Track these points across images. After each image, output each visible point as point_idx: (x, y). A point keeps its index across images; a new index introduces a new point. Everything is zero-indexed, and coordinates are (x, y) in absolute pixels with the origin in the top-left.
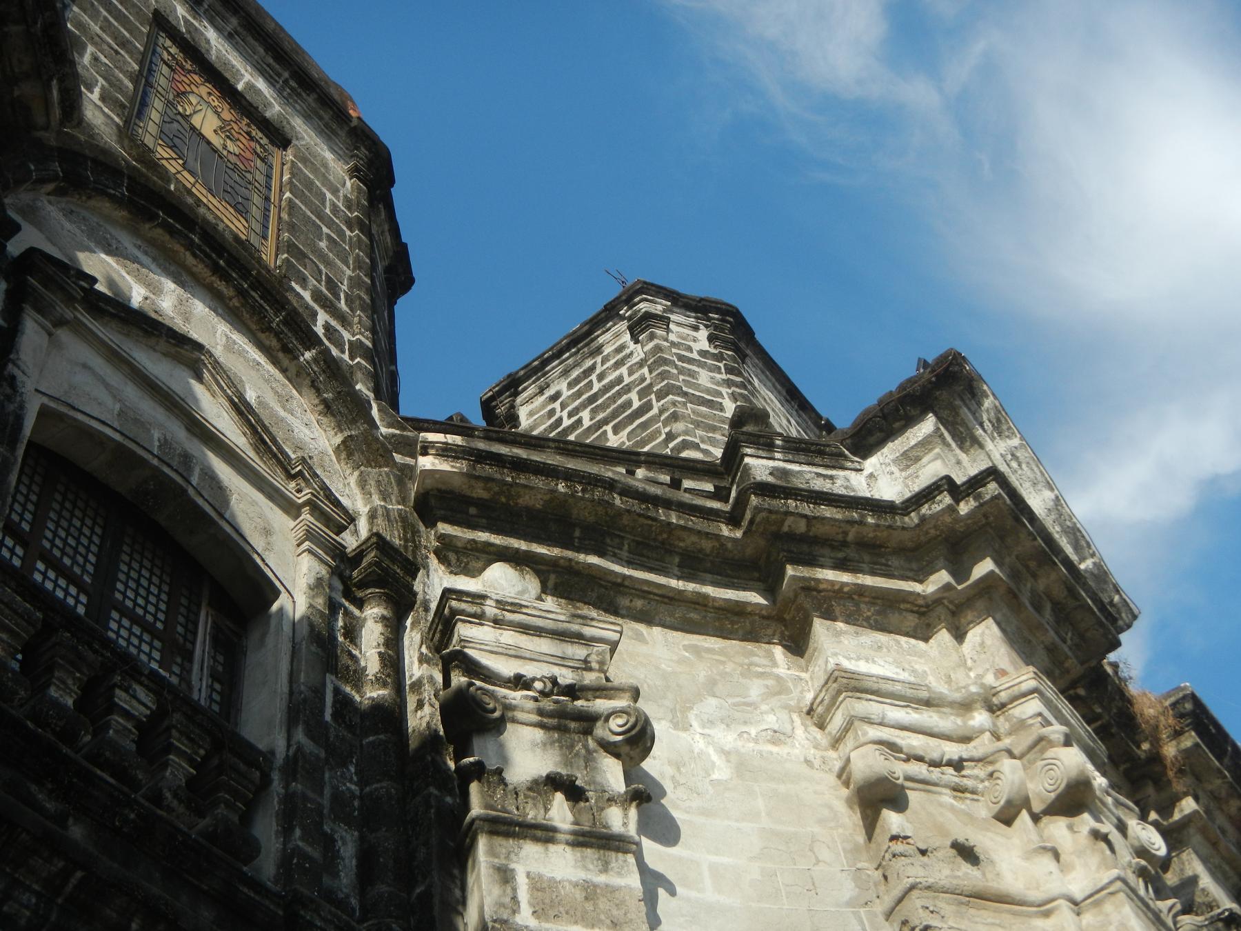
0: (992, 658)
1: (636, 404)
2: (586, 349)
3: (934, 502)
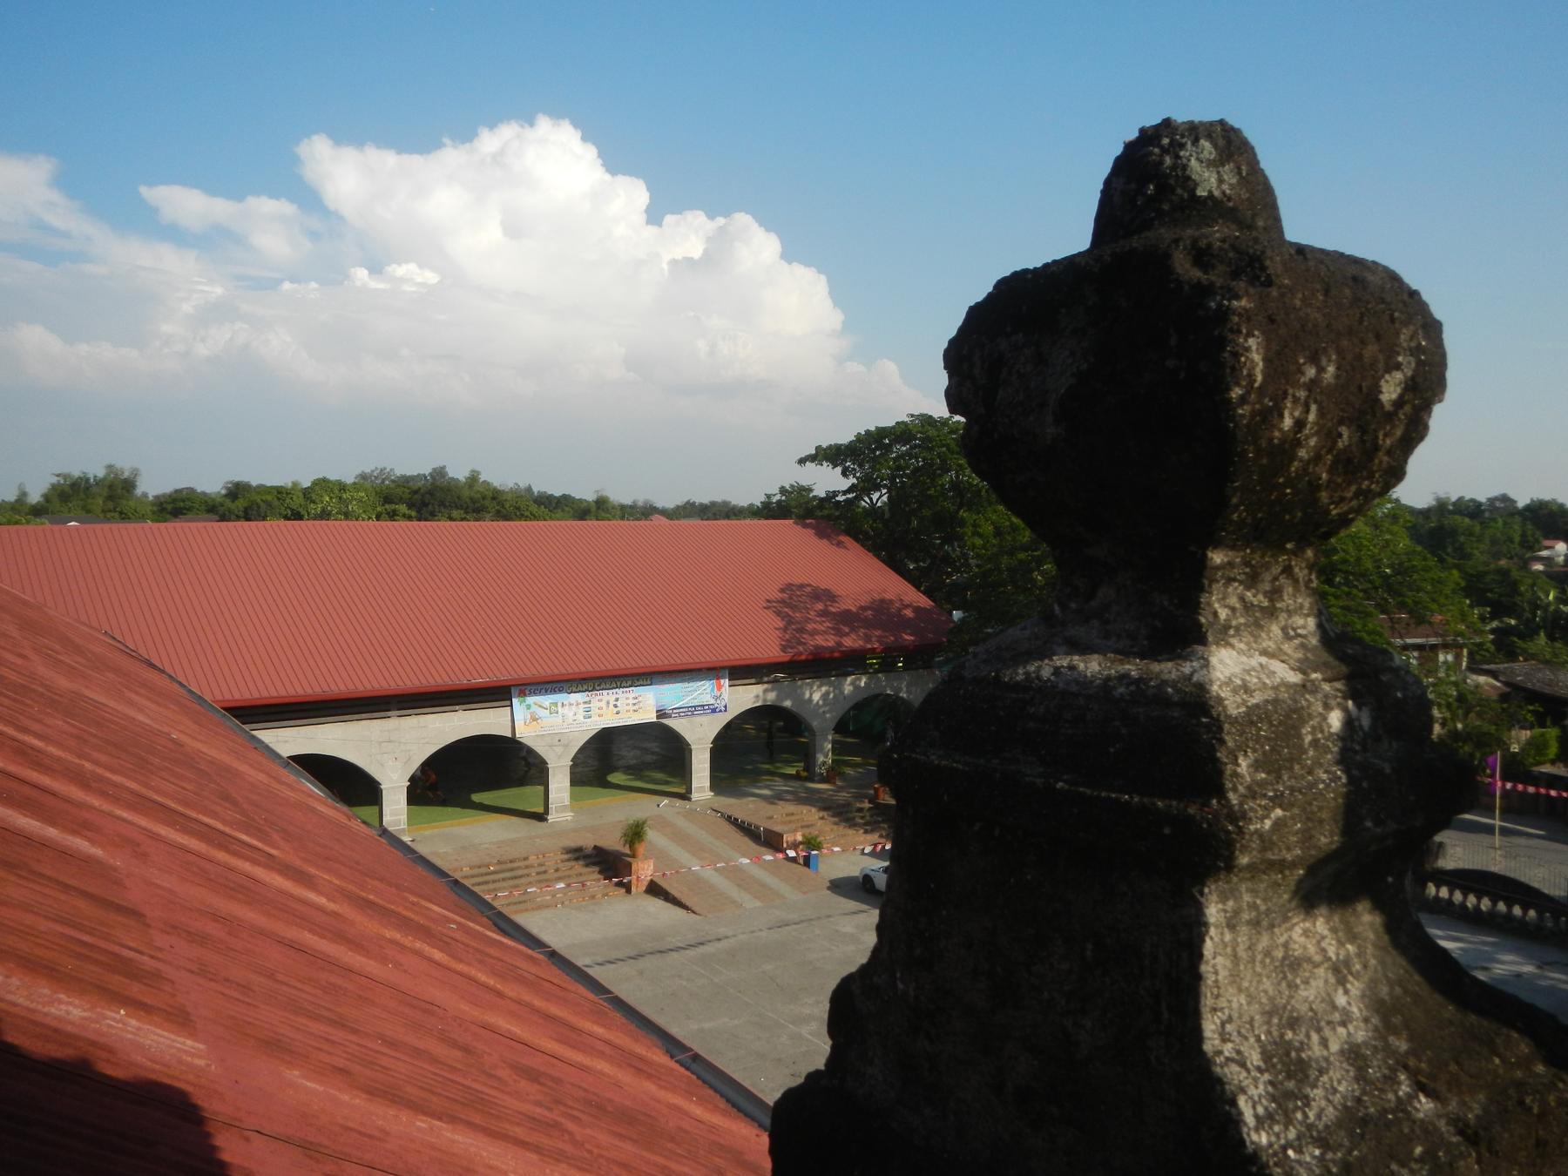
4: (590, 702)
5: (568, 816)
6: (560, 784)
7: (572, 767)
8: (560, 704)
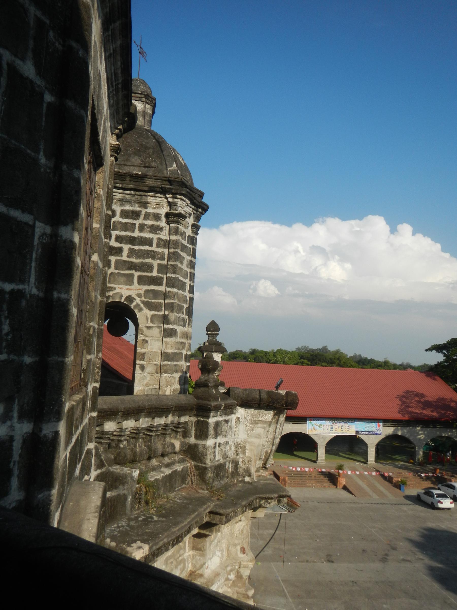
0: (243, 539)
1: (155, 273)
2: (139, 197)
3: (267, 501)
4: (333, 426)
5: (324, 463)
6: (321, 452)
7: (326, 447)
8: (323, 425)
